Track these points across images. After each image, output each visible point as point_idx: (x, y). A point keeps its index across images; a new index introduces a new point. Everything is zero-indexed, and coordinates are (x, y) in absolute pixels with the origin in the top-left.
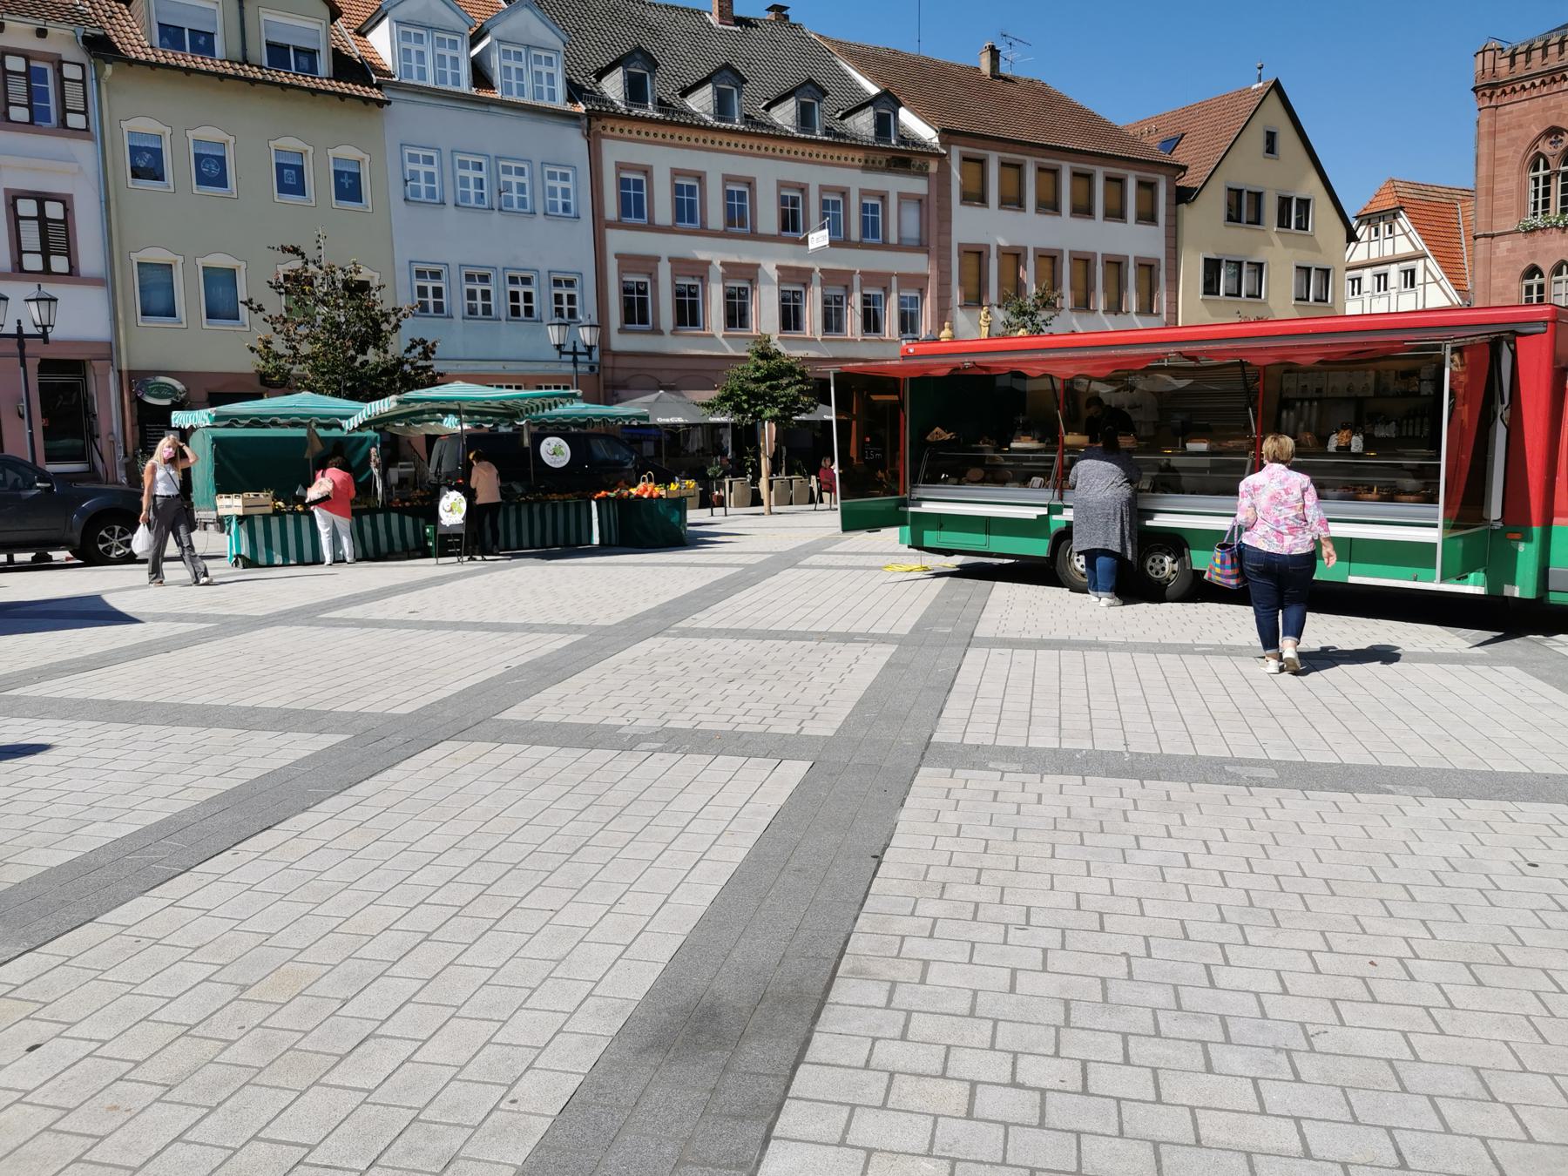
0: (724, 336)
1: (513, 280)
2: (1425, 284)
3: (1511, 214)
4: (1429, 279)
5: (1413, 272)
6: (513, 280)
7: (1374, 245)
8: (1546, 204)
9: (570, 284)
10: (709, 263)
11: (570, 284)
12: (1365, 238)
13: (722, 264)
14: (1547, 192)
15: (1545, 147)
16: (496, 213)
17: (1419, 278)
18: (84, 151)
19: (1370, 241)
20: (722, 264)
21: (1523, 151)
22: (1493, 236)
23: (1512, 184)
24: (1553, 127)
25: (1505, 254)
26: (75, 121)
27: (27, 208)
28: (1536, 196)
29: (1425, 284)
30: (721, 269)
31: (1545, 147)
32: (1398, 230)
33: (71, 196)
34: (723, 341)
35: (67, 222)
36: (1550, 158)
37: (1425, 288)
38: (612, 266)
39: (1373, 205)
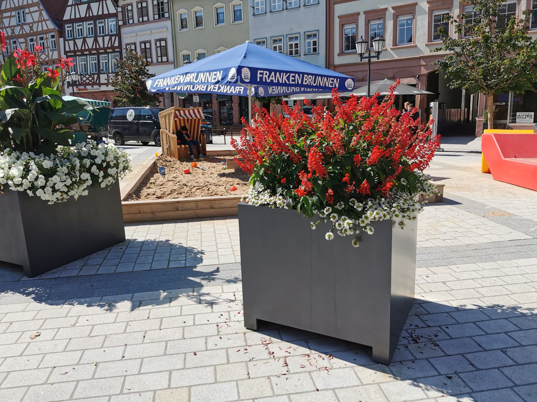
0: (391, 49)
1: (291, 39)
6: (291, 39)
9: (315, 35)
10: (386, 9)
11: (315, 35)
13: (393, 8)
16: (285, 11)
18: (168, 23)
20: (393, 8)
26: (166, 15)
27: (158, 43)
30: (393, 11)
33: (166, 38)
34: (392, 52)
35: (166, 46)
38: (337, 22)
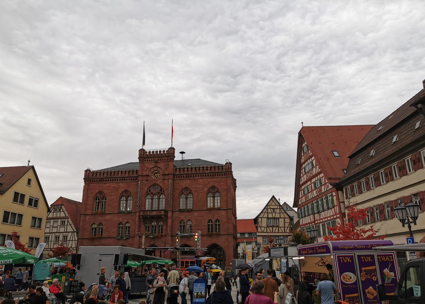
2: (67, 225)
3: (90, 210)
4: (68, 224)
5: (64, 222)
7: (55, 213)
8: (98, 208)
12: (53, 211)
14: (98, 206)
15: (98, 195)
17: (66, 224)
19: (54, 212)
21: (94, 195)
22: (85, 215)
23: (91, 203)
24: (101, 191)
25: (88, 219)
28: (96, 206)
29: (67, 225)
31: (98, 195)
32: (62, 210)
36: (99, 198)
37: (67, 226)
39: (56, 203)
